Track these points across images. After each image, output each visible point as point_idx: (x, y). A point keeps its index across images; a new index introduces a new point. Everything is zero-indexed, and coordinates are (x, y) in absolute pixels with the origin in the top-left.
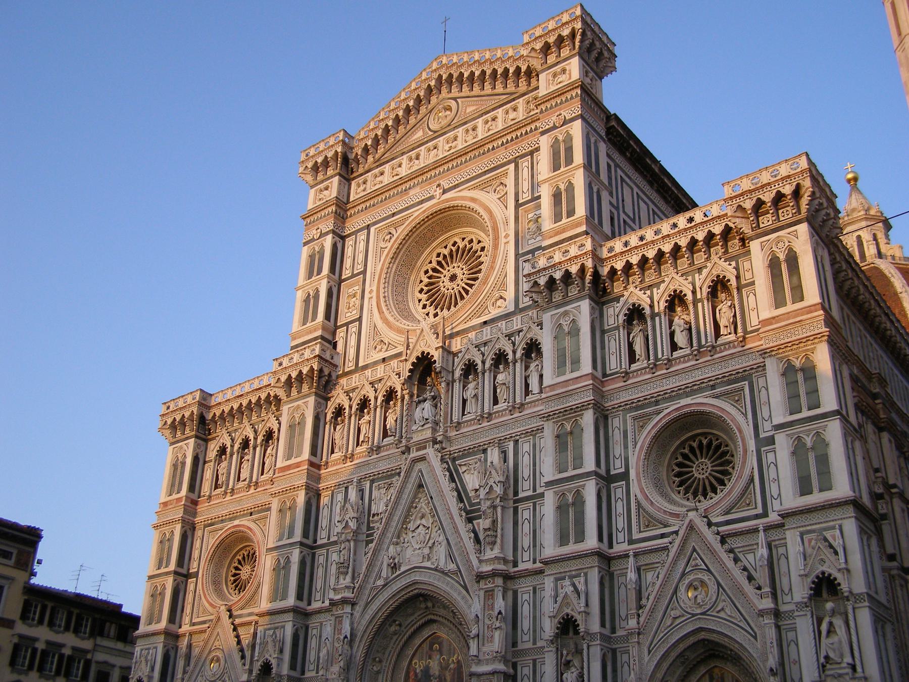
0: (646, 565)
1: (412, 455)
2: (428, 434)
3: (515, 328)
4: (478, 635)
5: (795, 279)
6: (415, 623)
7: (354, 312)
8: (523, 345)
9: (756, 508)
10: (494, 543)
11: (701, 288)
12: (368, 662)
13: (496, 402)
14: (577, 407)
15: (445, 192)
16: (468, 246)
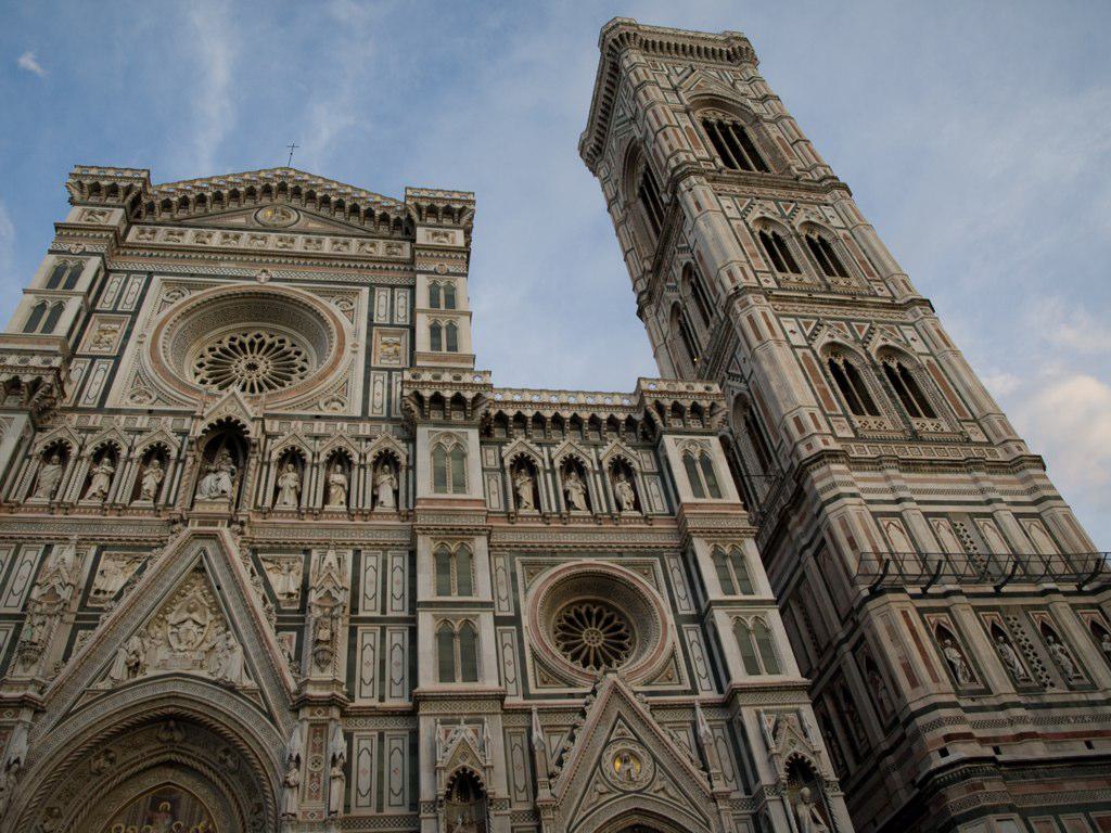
0: (551, 726)
1: (190, 528)
2: (224, 509)
3: (361, 433)
4: (298, 786)
5: (710, 479)
6: (138, 763)
7: (108, 349)
8: (375, 452)
9: (680, 684)
10: (328, 662)
11: (600, 463)
12: (39, 813)
13: (326, 500)
14: (468, 530)
15: (272, 279)
16: (277, 345)
